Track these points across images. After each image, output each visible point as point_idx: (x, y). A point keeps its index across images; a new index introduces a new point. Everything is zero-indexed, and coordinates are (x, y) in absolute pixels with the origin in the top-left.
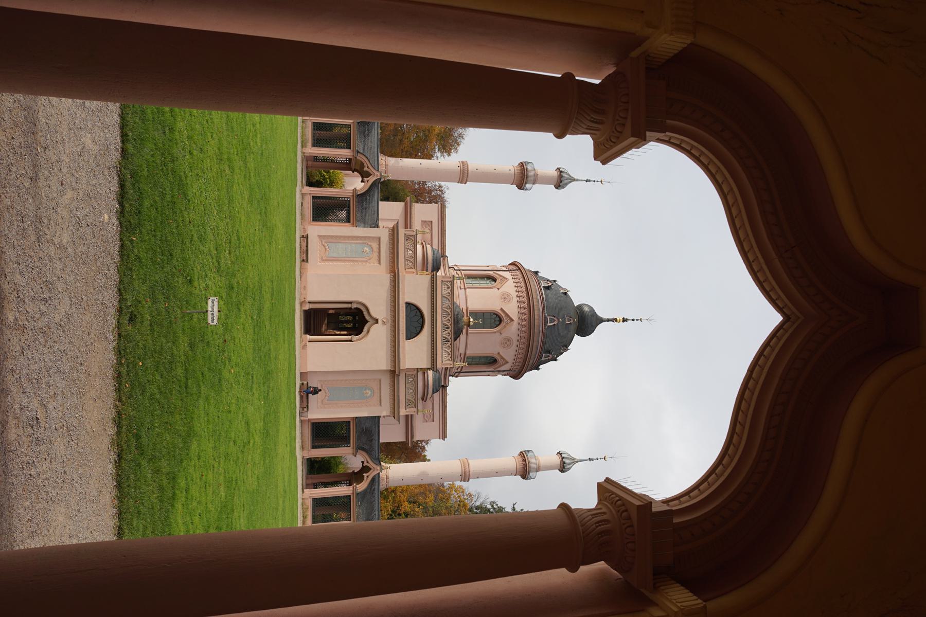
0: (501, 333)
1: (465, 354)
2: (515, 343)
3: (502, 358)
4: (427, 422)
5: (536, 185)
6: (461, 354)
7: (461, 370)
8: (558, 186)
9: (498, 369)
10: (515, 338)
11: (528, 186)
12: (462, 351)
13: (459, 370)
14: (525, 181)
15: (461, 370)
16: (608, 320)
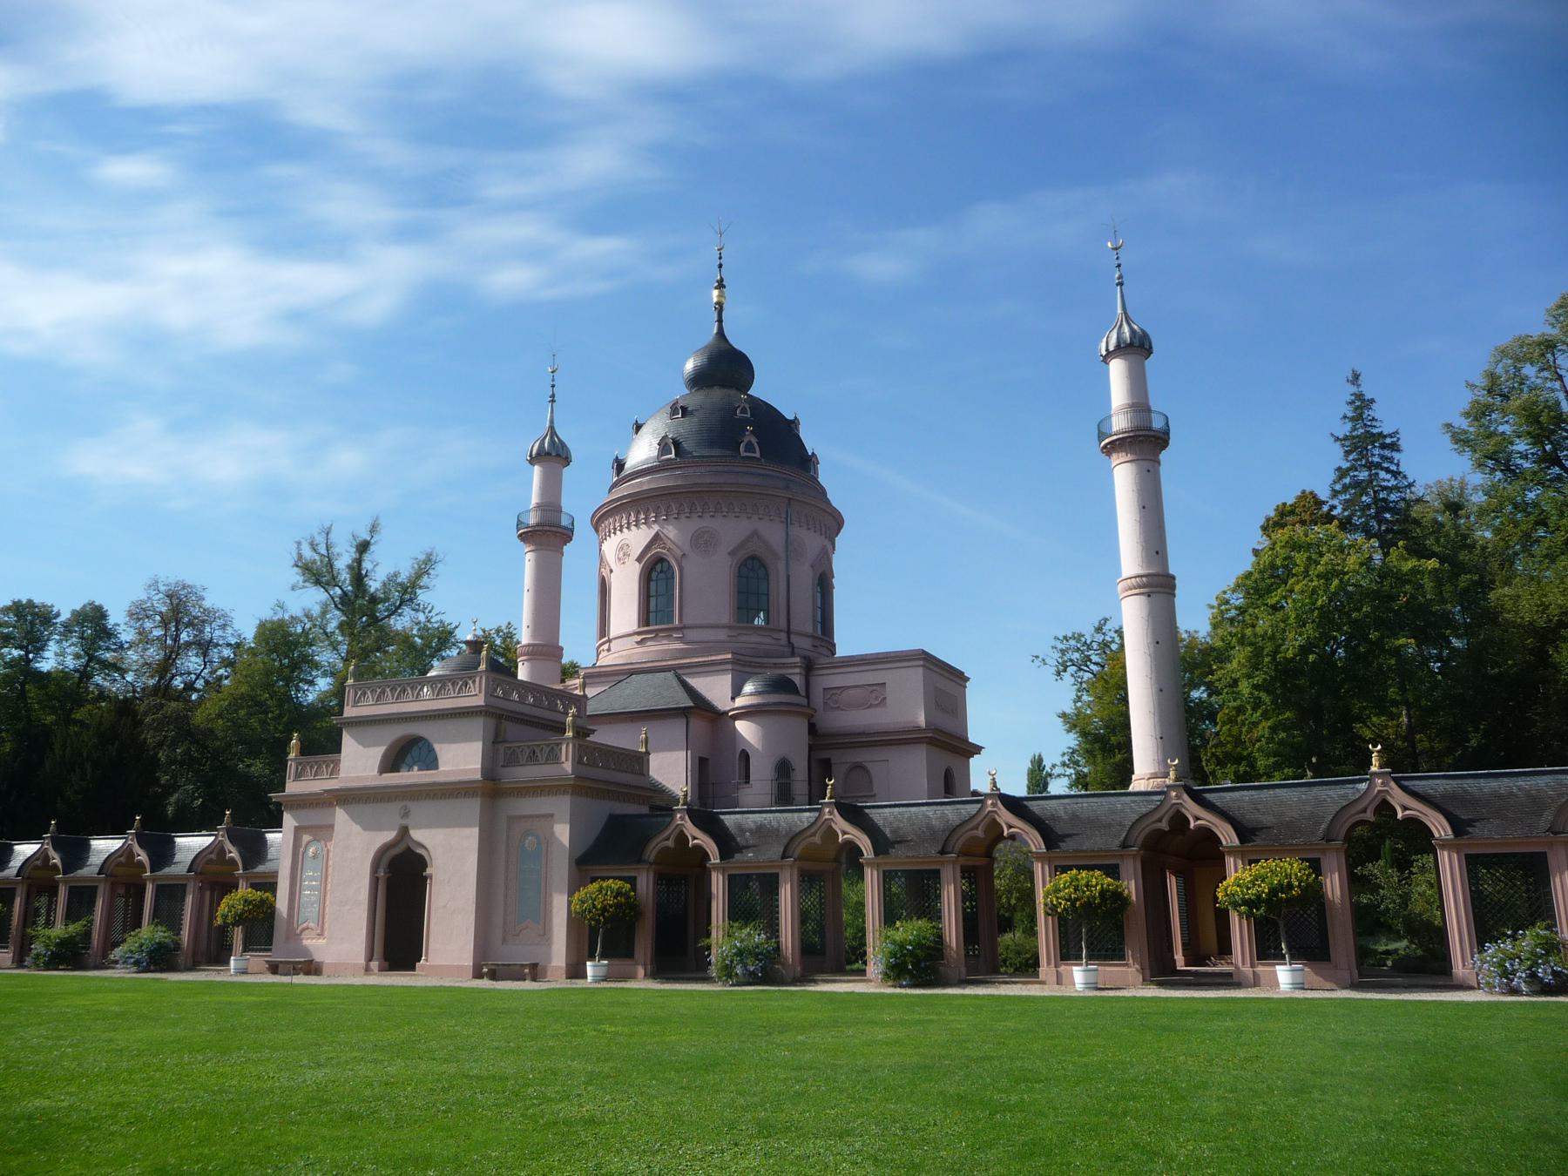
0: (684, 555)
1: (729, 627)
2: (707, 522)
3: (742, 544)
4: (885, 698)
5: (562, 505)
6: (729, 636)
7: (781, 631)
8: (566, 460)
9: (780, 550)
10: (695, 524)
11: (565, 522)
12: (722, 635)
13: (783, 636)
14: (545, 528)
15: (781, 631)
16: (720, 321)
